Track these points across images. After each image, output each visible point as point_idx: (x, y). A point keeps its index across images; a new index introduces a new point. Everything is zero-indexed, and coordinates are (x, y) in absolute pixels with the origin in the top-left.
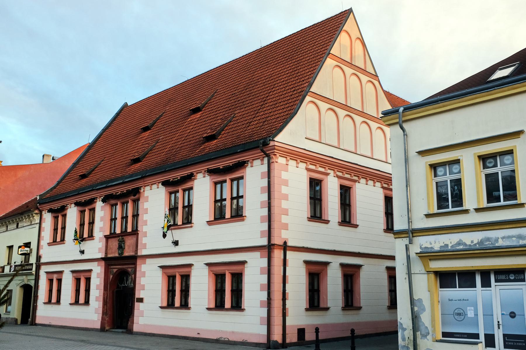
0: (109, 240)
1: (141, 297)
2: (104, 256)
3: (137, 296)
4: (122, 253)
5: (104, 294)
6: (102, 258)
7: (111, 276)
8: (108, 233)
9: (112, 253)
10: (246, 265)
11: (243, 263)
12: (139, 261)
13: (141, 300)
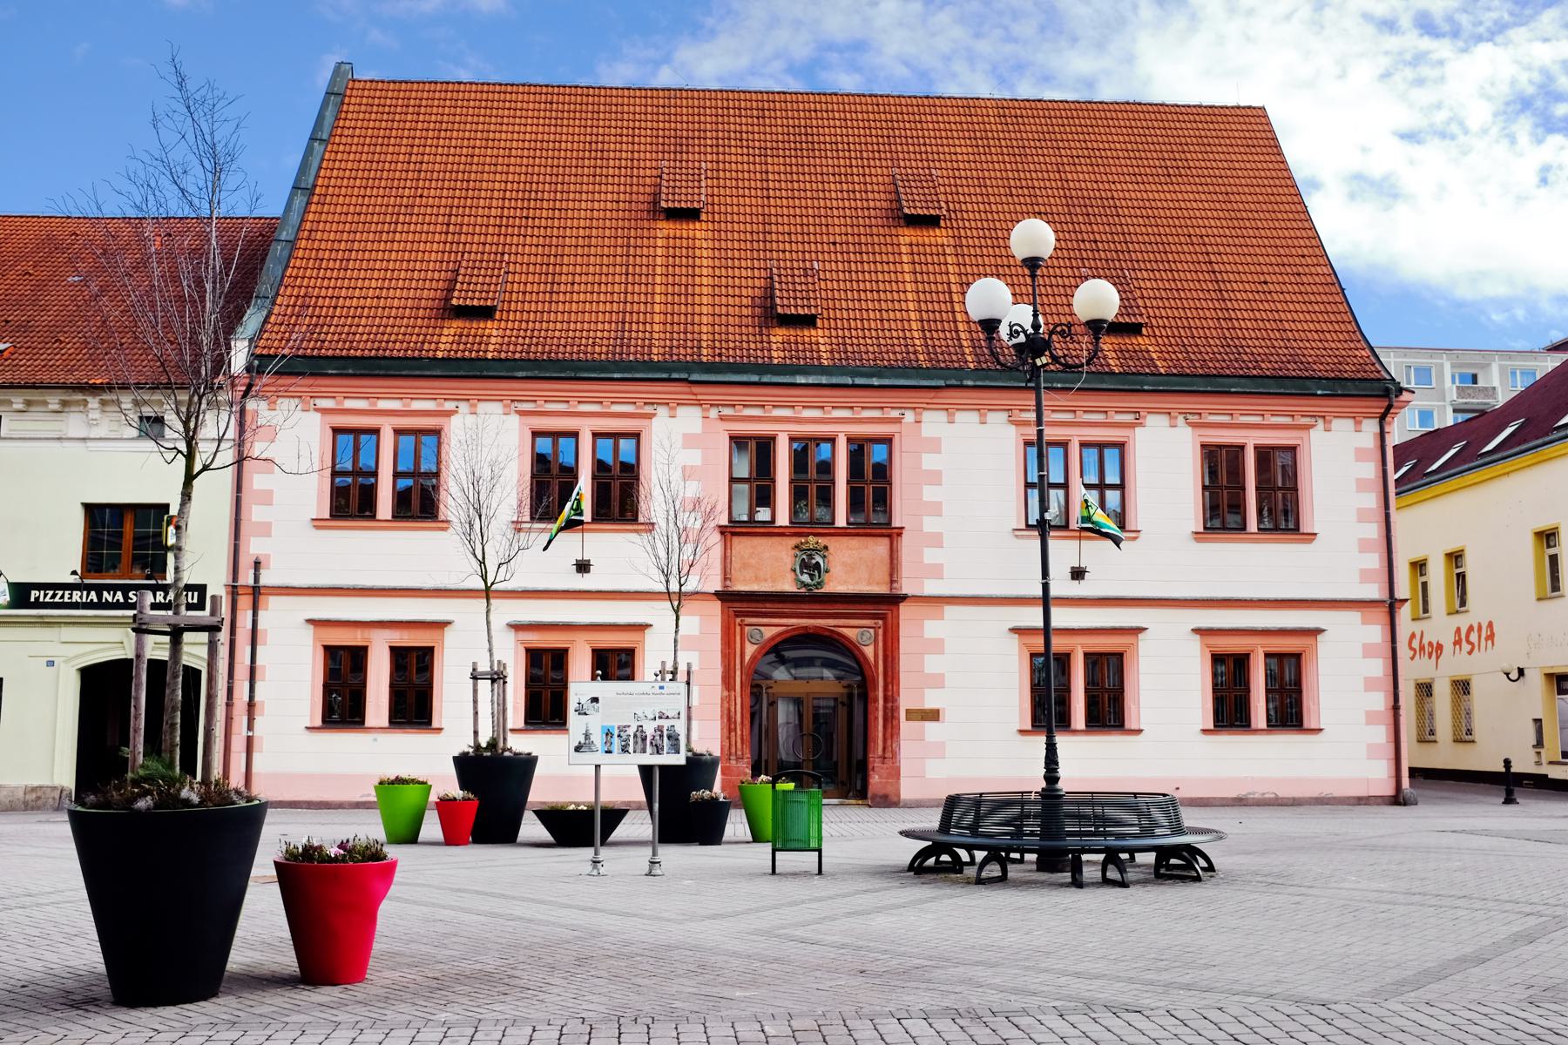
0: (736, 540)
1: (929, 704)
2: (719, 588)
3: (905, 702)
4: (820, 584)
5: (727, 701)
6: (717, 594)
7: (750, 650)
8: (724, 521)
9: (757, 579)
10: (1319, 637)
11: (1315, 632)
12: (904, 610)
13: (933, 715)
